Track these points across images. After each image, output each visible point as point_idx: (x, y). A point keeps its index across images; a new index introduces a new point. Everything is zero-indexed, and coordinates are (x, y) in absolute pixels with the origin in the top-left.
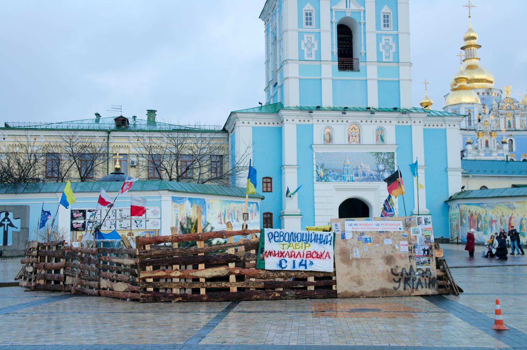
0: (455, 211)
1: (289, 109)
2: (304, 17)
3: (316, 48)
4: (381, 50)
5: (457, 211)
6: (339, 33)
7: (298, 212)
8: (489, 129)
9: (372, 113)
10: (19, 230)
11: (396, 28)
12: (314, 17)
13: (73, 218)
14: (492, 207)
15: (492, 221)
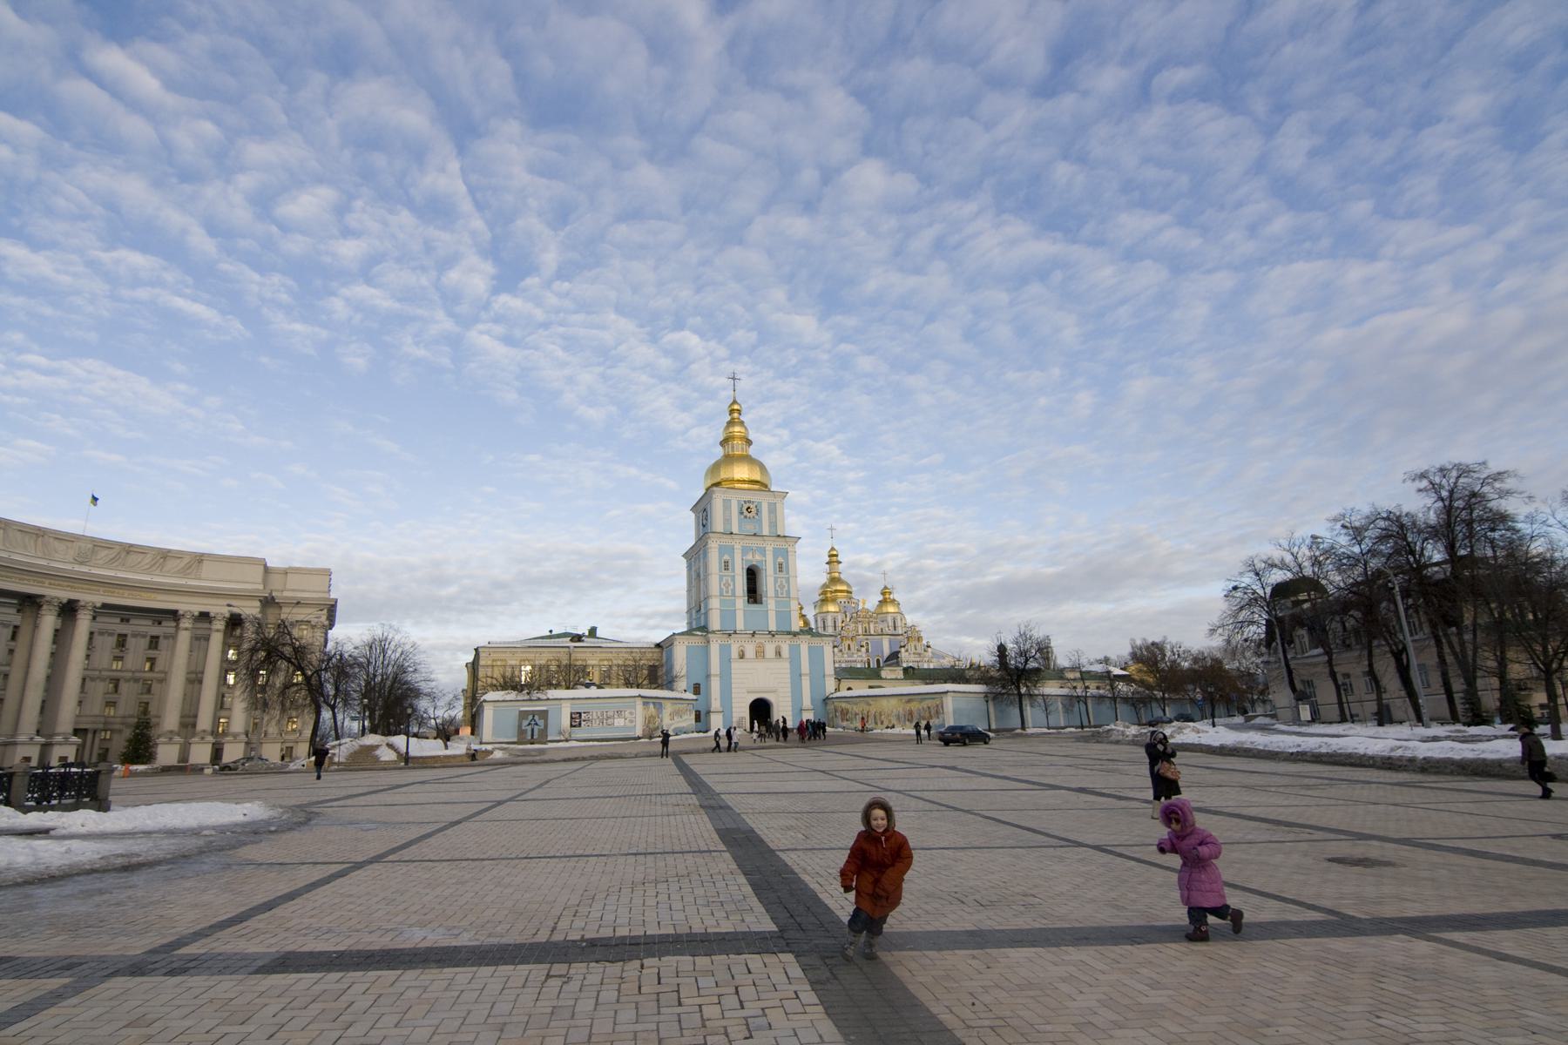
0: (831, 707)
1: (714, 632)
2: (723, 564)
3: (732, 587)
4: (777, 588)
5: (833, 707)
6: (748, 574)
7: (721, 710)
8: (851, 635)
9: (773, 636)
10: (542, 727)
11: (788, 573)
12: (730, 564)
13: (572, 718)
14: (856, 704)
15: (856, 714)
